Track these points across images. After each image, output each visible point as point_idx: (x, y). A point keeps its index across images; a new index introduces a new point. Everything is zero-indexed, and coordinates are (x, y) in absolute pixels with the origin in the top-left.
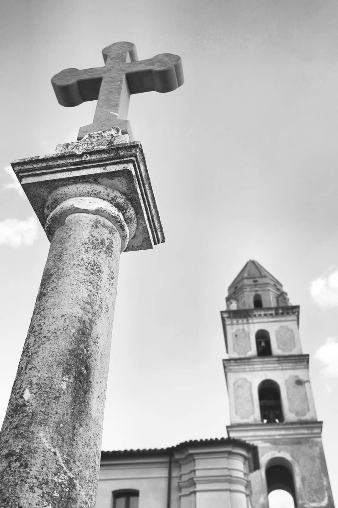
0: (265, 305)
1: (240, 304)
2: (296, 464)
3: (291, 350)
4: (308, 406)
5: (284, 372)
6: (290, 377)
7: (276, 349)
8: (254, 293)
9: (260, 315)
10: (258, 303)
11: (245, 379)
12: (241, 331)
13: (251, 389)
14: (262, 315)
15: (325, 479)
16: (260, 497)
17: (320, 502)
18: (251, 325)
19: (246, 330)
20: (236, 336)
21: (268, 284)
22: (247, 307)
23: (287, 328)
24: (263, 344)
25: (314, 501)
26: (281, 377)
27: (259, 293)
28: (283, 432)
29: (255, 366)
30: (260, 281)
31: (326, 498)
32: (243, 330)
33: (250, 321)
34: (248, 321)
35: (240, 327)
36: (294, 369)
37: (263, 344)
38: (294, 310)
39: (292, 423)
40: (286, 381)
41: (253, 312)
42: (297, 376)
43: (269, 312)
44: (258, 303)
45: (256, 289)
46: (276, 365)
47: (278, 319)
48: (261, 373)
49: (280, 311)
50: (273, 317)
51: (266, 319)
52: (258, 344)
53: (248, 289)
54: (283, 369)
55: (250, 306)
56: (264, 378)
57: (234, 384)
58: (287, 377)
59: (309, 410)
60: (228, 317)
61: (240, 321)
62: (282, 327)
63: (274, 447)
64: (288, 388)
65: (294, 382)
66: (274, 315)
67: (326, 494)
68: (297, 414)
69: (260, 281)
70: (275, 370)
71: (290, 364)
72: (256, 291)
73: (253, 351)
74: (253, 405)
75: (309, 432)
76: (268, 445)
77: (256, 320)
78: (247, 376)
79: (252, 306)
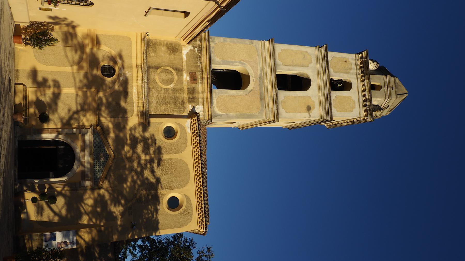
0: (373, 92)
2: (245, 93)
4: (290, 113)
5: (318, 98)
6: (314, 102)
7: (335, 94)
8: (382, 85)
11: (311, 62)
12: (350, 66)
15: (234, 115)
16: (220, 59)
17: (217, 107)
18: (356, 76)
19: (352, 71)
20: (346, 61)
21: (391, 98)
23: (353, 107)
24: (339, 86)
25: (217, 102)
26: (314, 93)
27: (383, 89)
28: (269, 87)
29: (321, 72)
30: (393, 92)
31: (220, 113)
32: (351, 69)
33: (359, 76)
34: (359, 74)
35: (354, 66)
36: (320, 106)
37: (339, 86)
38: (369, 116)
39: (277, 95)
40: (310, 97)
41: (367, 79)
42: (314, 108)
43: (367, 93)
45: (386, 87)
46: (323, 92)
48: (316, 77)
49: (368, 104)
51: (361, 89)
53: (386, 80)
54: (319, 96)
57: (307, 52)
58: (313, 99)
59: (287, 113)
61: (359, 67)
63: (258, 77)
65: (309, 104)
67: (223, 113)
68: (284, 102)
69: (393, 92)
70: (319, 89)
71: (324, 104)
72: (385, 87)
74: (290, 66)
75: (270, 109)
76: (259, 73)
77: (360, 80)
78: (313, 64)
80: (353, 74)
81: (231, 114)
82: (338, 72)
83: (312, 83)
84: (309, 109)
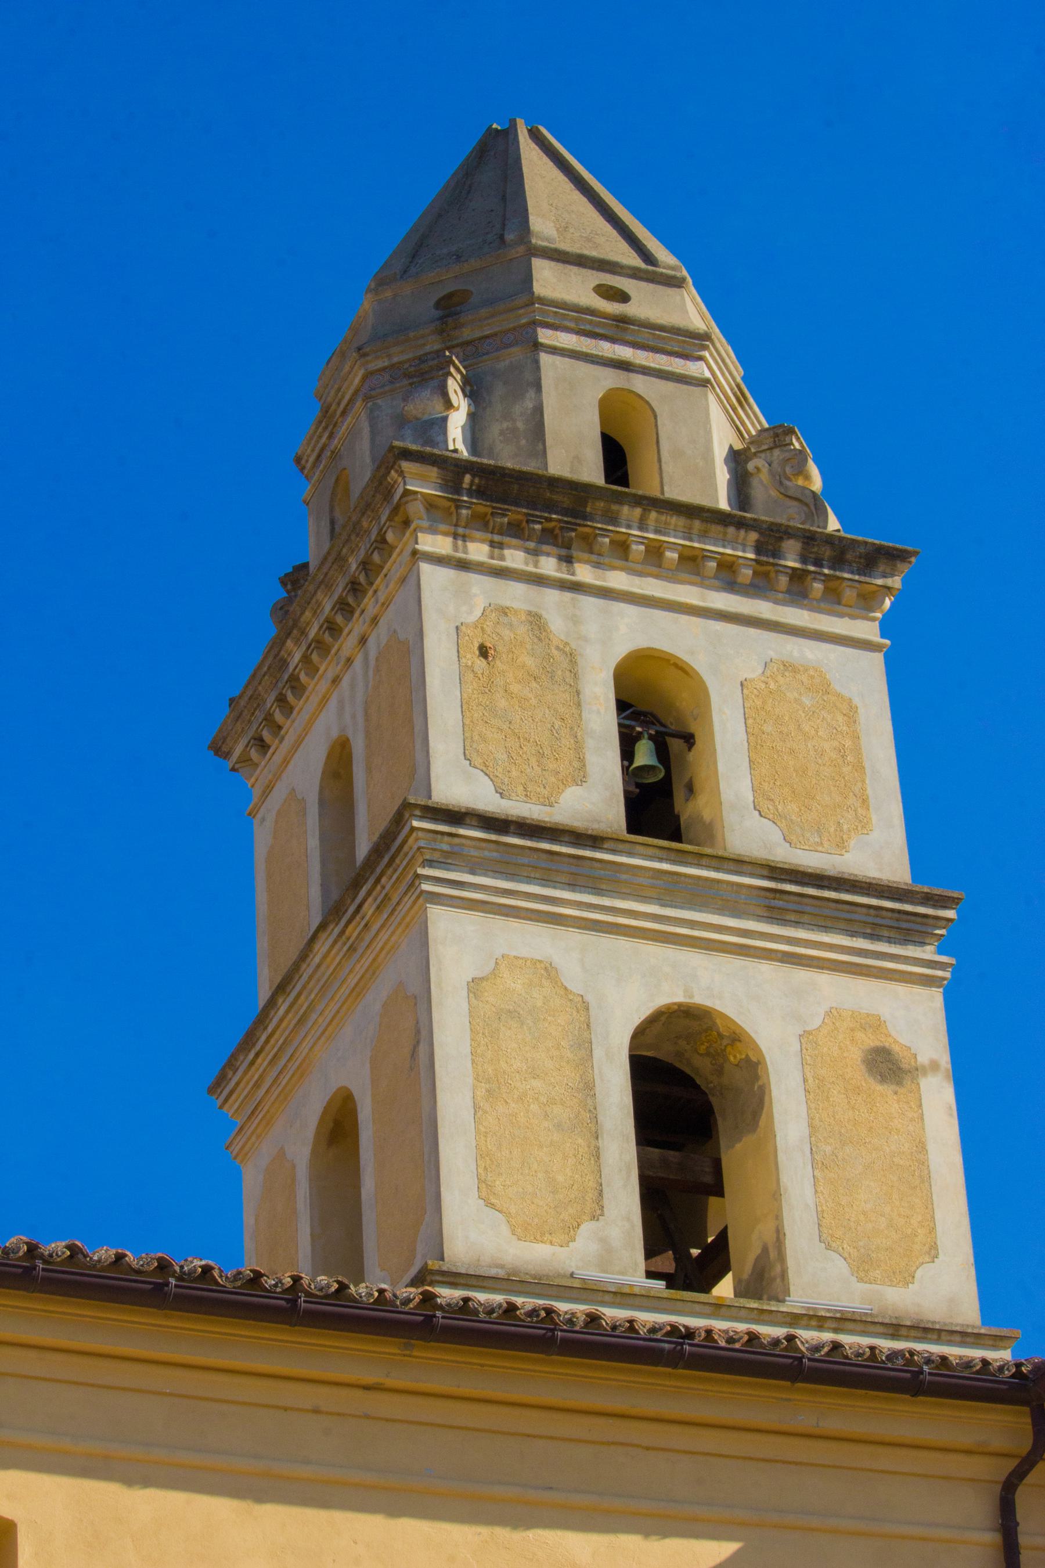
1: (495, 431)
3: (841, 845)
9: (655, 553)
11: (549, 971)
13: (584, 1046)
14: (672, 555)
19: (557, 625)
20: (484, 652)
22: (558, 466)
32: (536, 622)
35: (516, 595)
42: (875, 1024)
47: (763, 608)
56: (671, 995)
60: (430, 504)
62: (788, 667)
64: (815, 1091)
65: (856, 1055)
66: (746, 574)
80: (575, 620)
82: (578, 747)
83: (700, 999)
84: (886, 1065)
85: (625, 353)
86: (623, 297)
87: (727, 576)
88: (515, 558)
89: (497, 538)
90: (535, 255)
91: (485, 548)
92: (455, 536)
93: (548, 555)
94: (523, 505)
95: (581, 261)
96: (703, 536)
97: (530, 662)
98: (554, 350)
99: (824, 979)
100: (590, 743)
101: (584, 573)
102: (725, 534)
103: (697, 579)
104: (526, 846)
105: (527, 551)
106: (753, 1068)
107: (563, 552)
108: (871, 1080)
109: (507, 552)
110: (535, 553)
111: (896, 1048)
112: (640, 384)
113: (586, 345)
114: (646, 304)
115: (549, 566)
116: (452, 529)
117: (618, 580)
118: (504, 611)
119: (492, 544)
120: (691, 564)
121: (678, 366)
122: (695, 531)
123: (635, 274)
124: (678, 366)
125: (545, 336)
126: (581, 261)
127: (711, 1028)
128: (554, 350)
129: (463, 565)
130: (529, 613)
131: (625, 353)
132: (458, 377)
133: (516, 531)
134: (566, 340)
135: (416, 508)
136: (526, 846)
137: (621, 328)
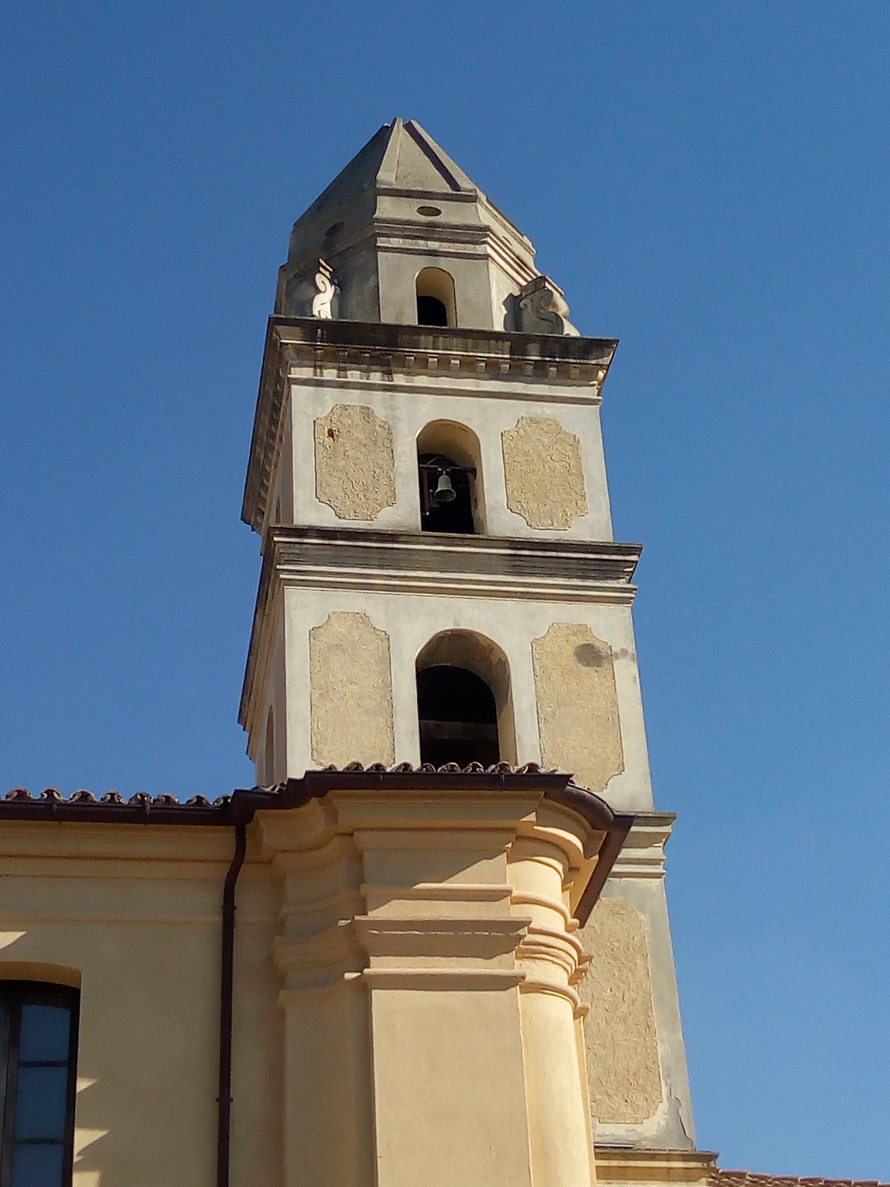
1: (353, 302)
7: (501, 510)
10: (433, 308)
22: (387, 318)
24: (443, 484)
37: (443, 484)
44: (433, 308)
50: (497, 377)
52: (427, 480)
55: (401, 313)
59: (621, 769)
65: (570, 650)
73: (403, 509)
79: (411, 318)
80: (392, 408)
81: (661, 1050)
85: (434, 245)
86: (437, 212)
87: (493, 371)
88: (354, 376)
89: (342, 365)
90: (380, 195)
91: (335, 372)
92: (315, 367)
93: (376, 371)
94: (362, 343)
95: (409, 194)
96: (475, 348)
97: (361, 436)
98: (386, 249)
99: (548, 605)
100: (399, 481)
101: (399, 379)
102: (489, 345)
103: (474, 375)
104: (357, 549)
105: (361, 371)
106: (503, 664)
107: (385, 369)
108: (579, 665)
109: (349, 373)
110: (368, 371)
111: (597, 644)
112: (444, 263)
113: (409, 244)
114: (451, 214)
115: (376, 378)
116: (313, 363)
117: (421, 381)
118: (345, 408)
119: (340, 369)
120: (468, 367)
121: (469, 249)
122: (470, 346)
123: (446, 197)
124: (469, 249)
125: (381, 242)
126: (409, 194)
127: (477, 643)
128: (386, 249)
129: (320, 384)
130: (362, 407)
131: (434, 245)
132: (327, 274)
133: (355, 360)
134: (395, 242)
135: (289, 353)
136: (357, 549)
137: (430, 231)
